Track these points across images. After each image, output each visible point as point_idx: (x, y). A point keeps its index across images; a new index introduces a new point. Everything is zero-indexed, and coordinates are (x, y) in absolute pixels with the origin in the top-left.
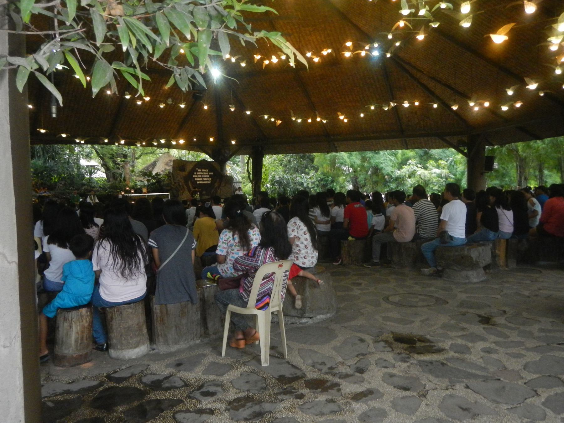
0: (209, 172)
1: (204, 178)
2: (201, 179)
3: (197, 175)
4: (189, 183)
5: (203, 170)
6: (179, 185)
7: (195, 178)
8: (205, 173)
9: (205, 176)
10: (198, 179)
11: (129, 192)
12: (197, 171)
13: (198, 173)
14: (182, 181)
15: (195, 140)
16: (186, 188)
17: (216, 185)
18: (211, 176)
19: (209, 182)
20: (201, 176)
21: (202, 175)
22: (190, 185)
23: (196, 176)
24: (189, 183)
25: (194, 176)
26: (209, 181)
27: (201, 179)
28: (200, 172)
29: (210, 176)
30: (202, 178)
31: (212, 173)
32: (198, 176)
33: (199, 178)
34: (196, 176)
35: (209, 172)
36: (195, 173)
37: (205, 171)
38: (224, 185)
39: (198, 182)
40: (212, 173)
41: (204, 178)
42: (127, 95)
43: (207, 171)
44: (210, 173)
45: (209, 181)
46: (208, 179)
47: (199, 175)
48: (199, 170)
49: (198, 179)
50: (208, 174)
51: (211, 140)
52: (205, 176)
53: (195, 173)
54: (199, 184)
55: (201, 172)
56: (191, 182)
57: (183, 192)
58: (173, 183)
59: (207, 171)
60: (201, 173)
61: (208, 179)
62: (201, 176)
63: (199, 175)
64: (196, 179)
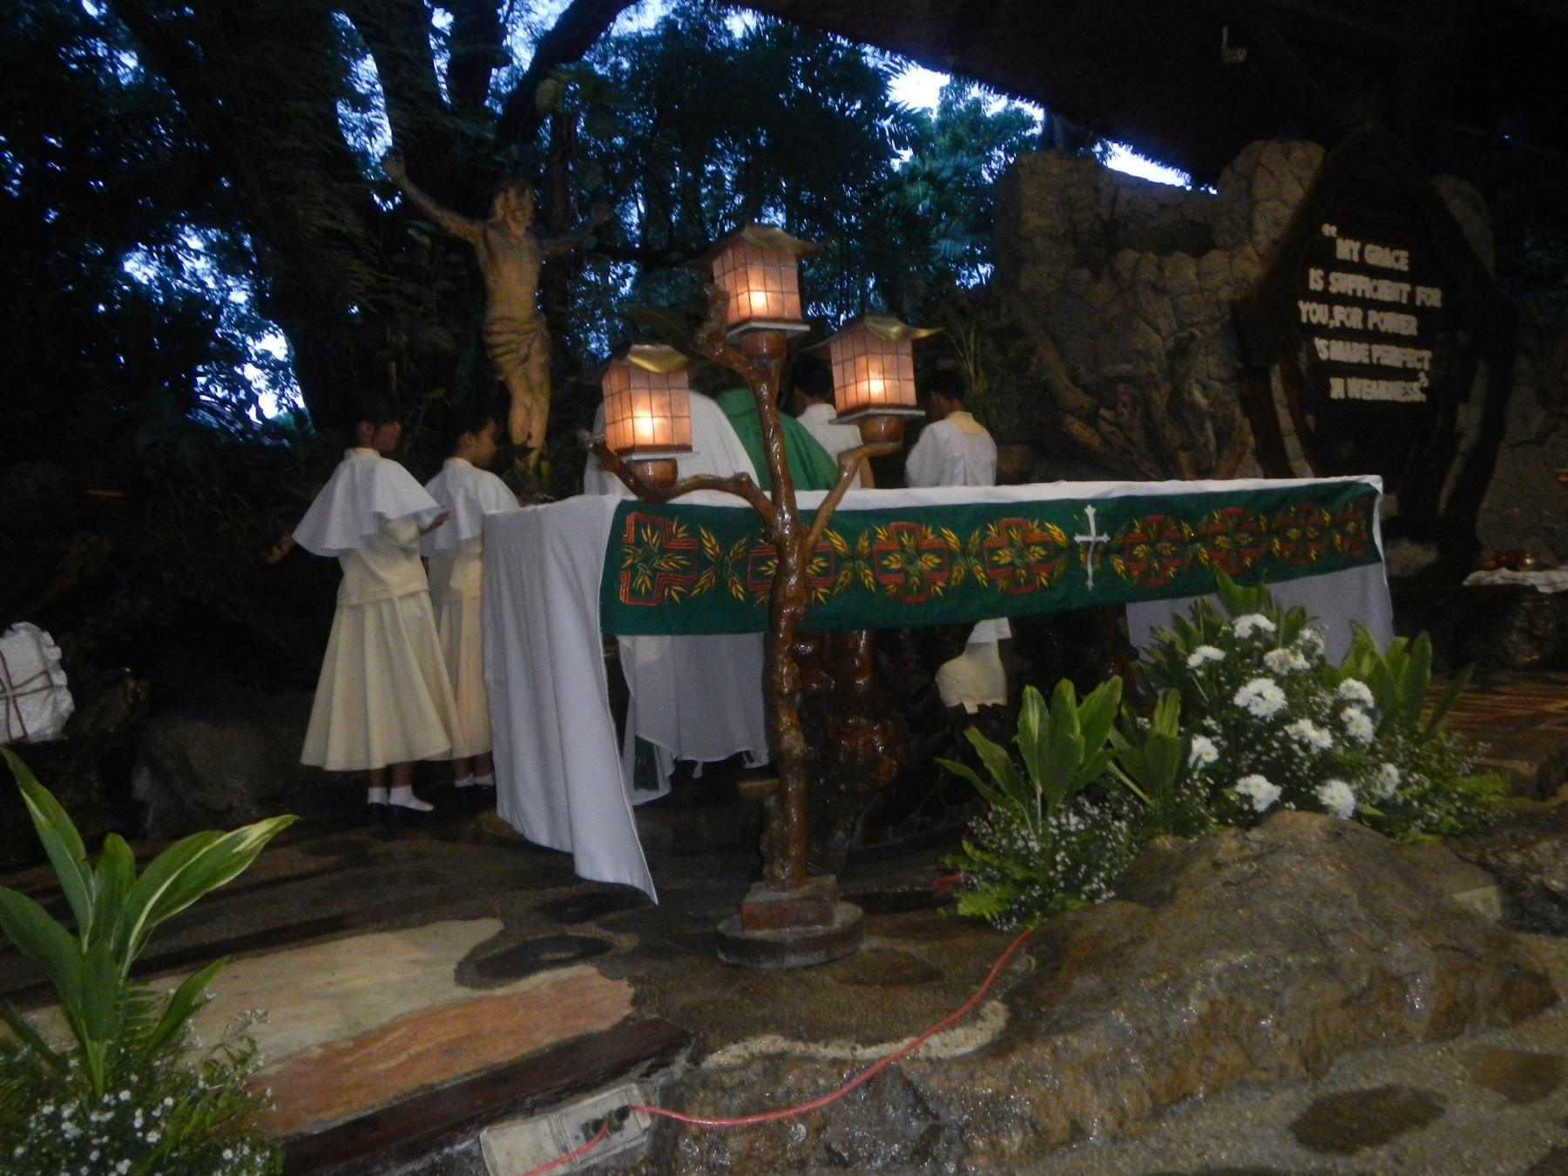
4: (1276, 384)
5: (1378, 255)
13: (1344, 283)
17: (1469, 418)
19: (1414, 392)
21: (1366, 304)
22: (1285, 421)
24: (1276, 384)
29: (1422, 313)
38: (1538, 419)
39: (1337, 388)
40: (1431, 297)
48: (1346, 249)
53: (1315, 278)
54: (1349, 403)
56: (1291, 380)
58: (1075, 397)
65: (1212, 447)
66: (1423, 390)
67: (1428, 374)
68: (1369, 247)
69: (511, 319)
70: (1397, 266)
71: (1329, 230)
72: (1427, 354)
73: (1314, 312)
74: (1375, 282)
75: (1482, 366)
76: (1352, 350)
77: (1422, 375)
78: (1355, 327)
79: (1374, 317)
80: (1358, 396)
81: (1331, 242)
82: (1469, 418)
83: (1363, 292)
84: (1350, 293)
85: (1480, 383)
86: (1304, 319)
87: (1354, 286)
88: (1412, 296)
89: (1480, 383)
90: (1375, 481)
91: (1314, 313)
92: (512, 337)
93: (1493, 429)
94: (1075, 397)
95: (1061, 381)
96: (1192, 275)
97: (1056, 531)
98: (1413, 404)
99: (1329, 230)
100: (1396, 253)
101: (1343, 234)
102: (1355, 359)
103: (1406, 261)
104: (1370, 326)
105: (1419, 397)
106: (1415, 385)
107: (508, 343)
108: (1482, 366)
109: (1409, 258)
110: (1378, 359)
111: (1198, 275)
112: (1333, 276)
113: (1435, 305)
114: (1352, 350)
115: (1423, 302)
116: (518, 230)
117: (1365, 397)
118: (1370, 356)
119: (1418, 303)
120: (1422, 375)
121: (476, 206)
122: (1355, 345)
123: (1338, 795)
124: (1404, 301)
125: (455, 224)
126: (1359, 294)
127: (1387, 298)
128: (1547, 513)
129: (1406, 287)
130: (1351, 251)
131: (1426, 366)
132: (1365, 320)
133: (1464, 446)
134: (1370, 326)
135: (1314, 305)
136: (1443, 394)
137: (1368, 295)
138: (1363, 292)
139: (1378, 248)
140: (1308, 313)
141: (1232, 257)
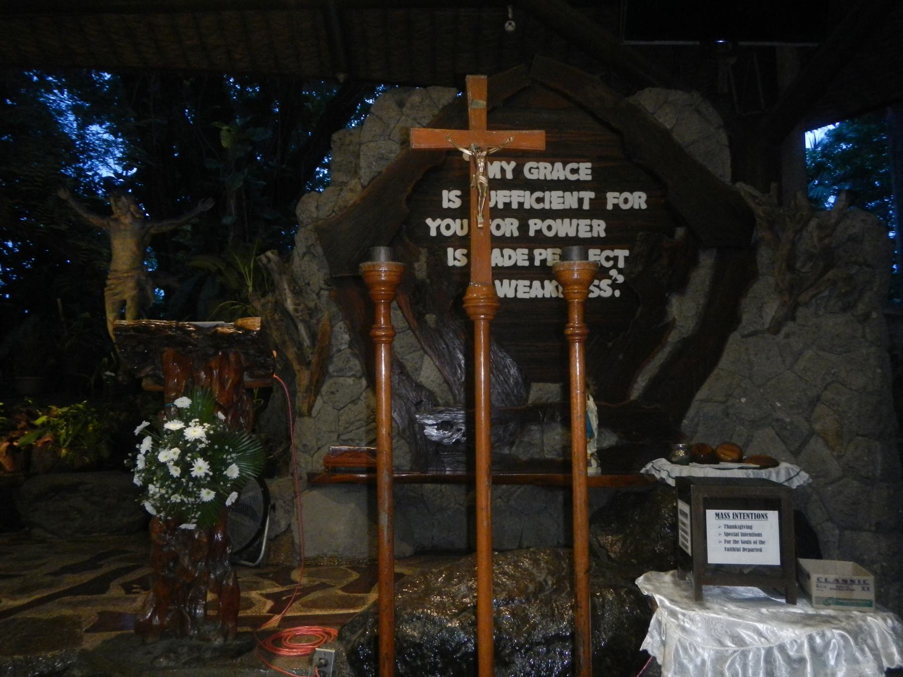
1: (541, 241)
2: (519, 257)
7: (442, 242)
8: (555, 200)
21: (523, 215)
25: (432, 225)
27: (519, 257)
30: (522, 240)
31: (638, 200)
36: (451, 199)
37: (559, 172)
38: (771, 310)
40: (638, 200)
41: (541, 241)
43: (585, 171)
44: (612, 199)
50: (597, 210)
53: (451, 199)
55: (519, 182)
57: (315, 388)
59: (585, 171)
60: (516, 197)
62: (510, 227)
64: (455, 258)
65: (307, 342)
66: (614, 285)
67: (620, 271)
69: (116, 271)
70: (573, 177)
72: (622, 254)
73: (448, 227)
74: (539, 194)
75: (707, 261)
76: (502, 256)
77: (613, 273)
78: (508, 235)
79: (535, 225)
80: (511, 295)
83: (521, 204)
84: (500, 206)
86: (433, 233)
87: (507, 200)
92: (115, 281)
96: (313, 209)
100: (574, 165)
102: (508, 263)
103: (589, 171)
104: (532, 233)
105: (607, 293)
106: (605, 283)
107: (112, 284)
108: (707, 261)
109: (592, 169)
110: (543, 262)
111: (317, 207)
113: (636, 207)
114: (502, 256)
115: (616, 206)
117: (520, 295)
118: (531, 258)
119: (610, 207)
120: (613, 273)
122: (507, 252)
124: (586, 206)
126: (515, 206)
127: (555, 206)
128: (779, 405)
129: (588, 195)
130: (503, 171)
131: (621, 264)
133: (673, 338)
134: (532, 233)
135: (448, 221)
137: (527, 206)
138: (521, 204)
139: (542, 165)
140: (438, 228)
141: (341, 190)
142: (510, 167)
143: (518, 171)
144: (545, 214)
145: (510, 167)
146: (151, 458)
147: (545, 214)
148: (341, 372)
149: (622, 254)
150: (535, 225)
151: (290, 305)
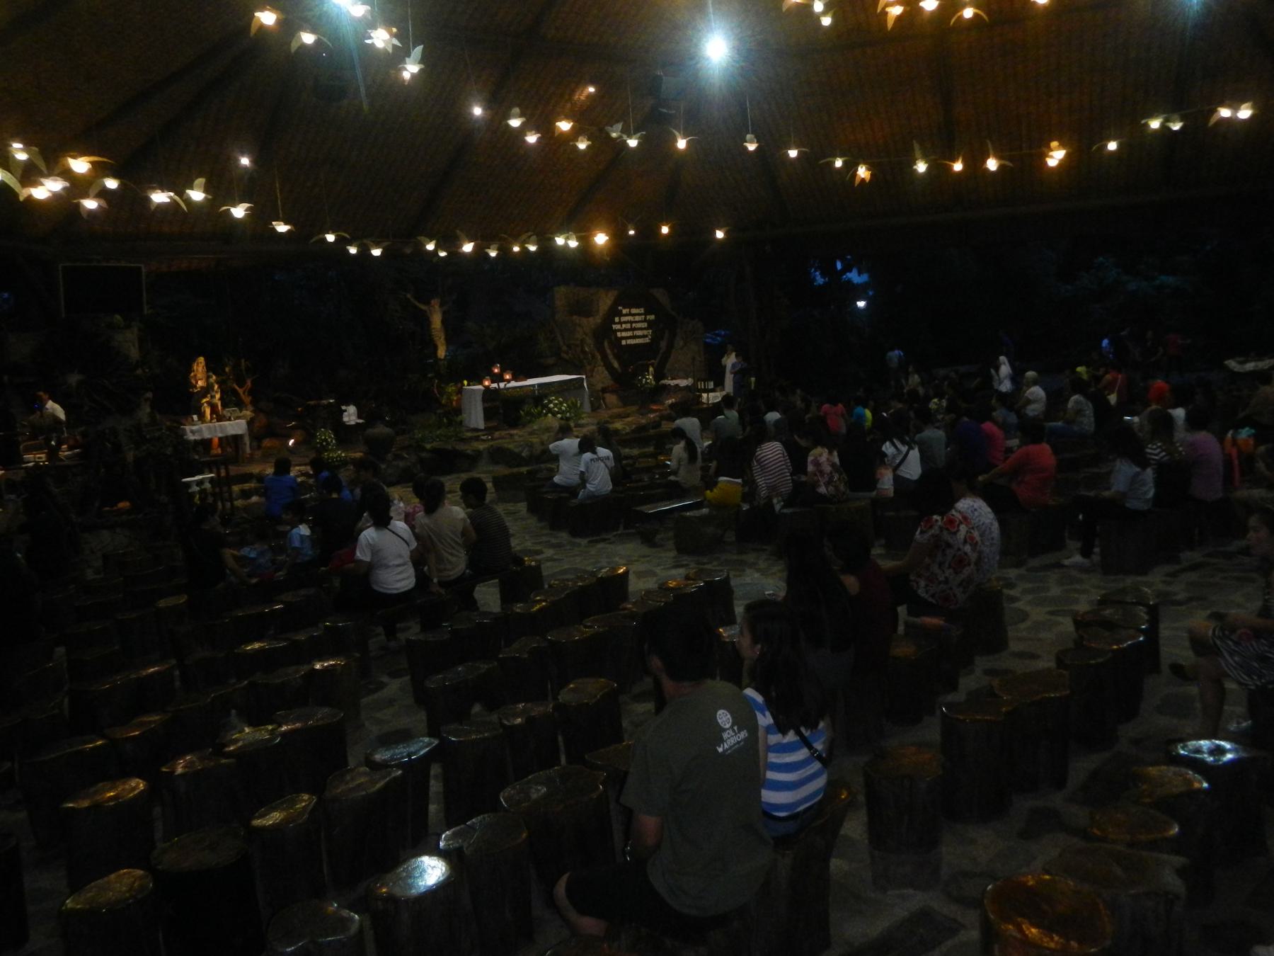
0: (645, 314)
1: (635, 329)
2: (629, 334)
3: (620, 323)
4: (606, 344)
5: (634, 311)
6: (583, 352)
8: (637, 318)
9: (639, 325)
10: (624, 334)
11: (499, 378)
12: (620, 314)
13: (624, 319)
14: (589, 341)
15: (632, 232)
16: (599, 357)
17: (663, 344)
18: (651, 325)
19: (647, 340)
20: (628, 326)
21: (631, 322)
22: (609, 351)
23: (618, 327)
24: (606, 344)
25: (614, 326)
26: (646, 336)
27: (629, 334)
28: (626, 315)
29: (649, 322)
30: (633, 329)
31: (652, 317)
32: (624, 326)
33: (626, 330)
34: (618, 327)
35: (645, 314)
36: (617, 319)
38: (681, 343)
39: (624, 342)
40: (652, 317)
41: (635, 329)
42: (515, 117)
43: (642, 311)
44: (648, 317)
45: (646, 336)
46: (645, 332)
47: (625, 323)
48: (625, 311)
49: (624, 334)
50: (645, 321)
51: (665, 230)
52: (639, 325)
53: (617, 319)
55: (630, 314)
58: (565, 348)
61: (645, 332)
62: (628, 326)
63: (625, 323)
64: (619, 334)
68: (632, 310)
71: (620, 308)
72: (650, 331)
79: (634, 325)
81: (621, 311)
82: (663, 344)
85: (667, 335)
88: (645, 318)
89: (667, 335)
90: (584, 377)
91: (615, 327)
93: (670, 346)
94: (565, 348)
95: (561, 343)
97: (532, 388)
98: (647, 343)
99: (620, 308)
101: (624, 308)
102: (629, 335)
112: (622, 318)
116: (437, 307)
121: (428, 303)
123: (559, 416)
125: (423, 307)
129: (643, 317)
132: (631, 325)
133: (661, 351)
136: (655, 340)
139: (634, 309)
142: (628, 310)
143: (630, 311)
144: (636, 322)
145: (628, 310)
146: (646, 382)
147: (636, 322)
148: (599, 366)
149: (650, 331)
150: (634, 325)
151: (587, 349)
